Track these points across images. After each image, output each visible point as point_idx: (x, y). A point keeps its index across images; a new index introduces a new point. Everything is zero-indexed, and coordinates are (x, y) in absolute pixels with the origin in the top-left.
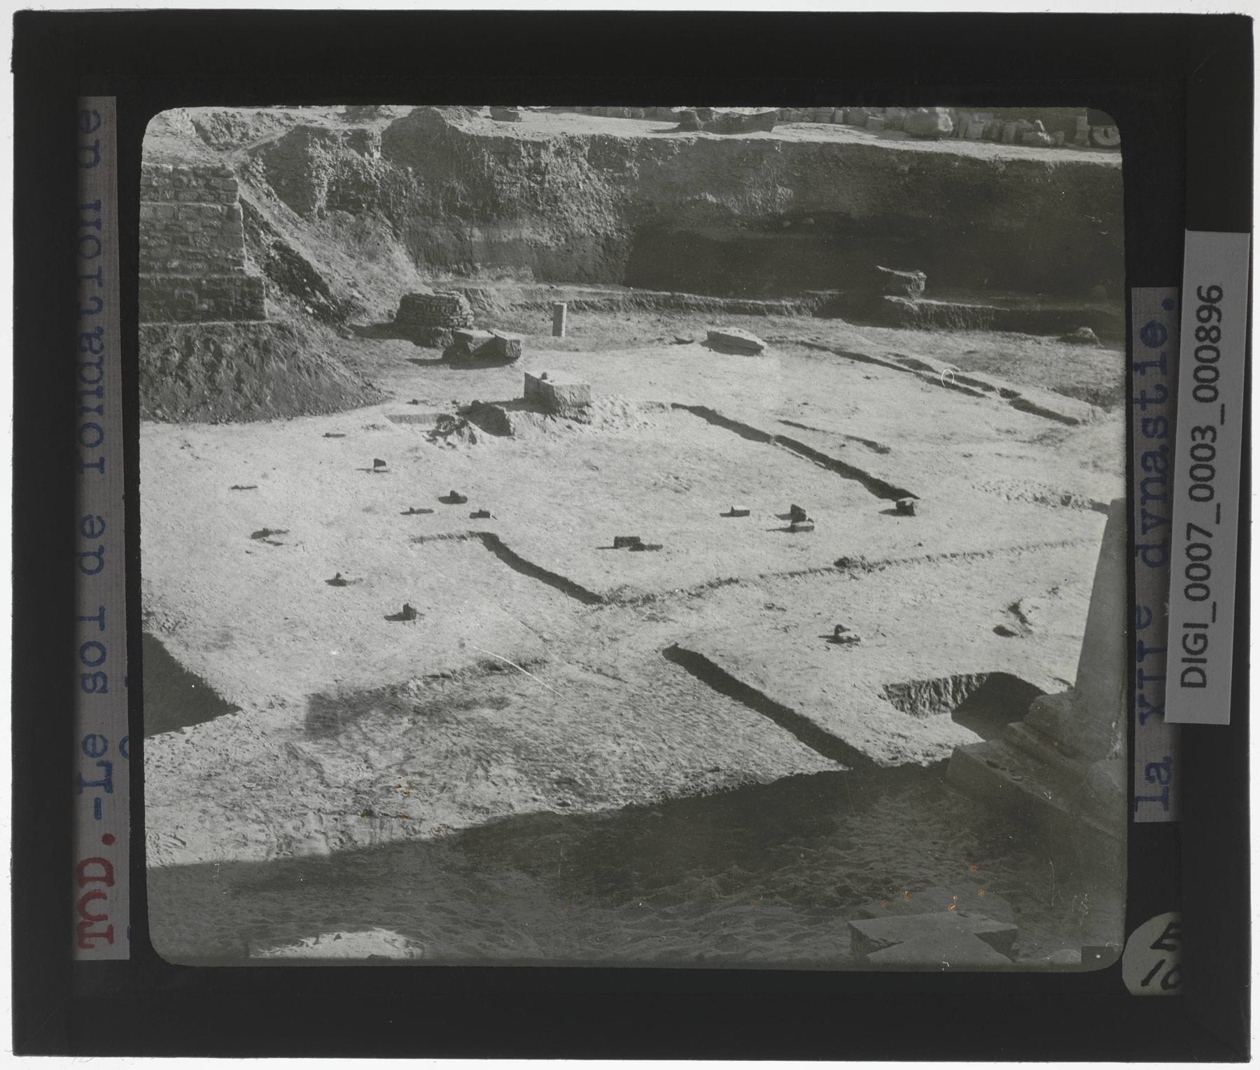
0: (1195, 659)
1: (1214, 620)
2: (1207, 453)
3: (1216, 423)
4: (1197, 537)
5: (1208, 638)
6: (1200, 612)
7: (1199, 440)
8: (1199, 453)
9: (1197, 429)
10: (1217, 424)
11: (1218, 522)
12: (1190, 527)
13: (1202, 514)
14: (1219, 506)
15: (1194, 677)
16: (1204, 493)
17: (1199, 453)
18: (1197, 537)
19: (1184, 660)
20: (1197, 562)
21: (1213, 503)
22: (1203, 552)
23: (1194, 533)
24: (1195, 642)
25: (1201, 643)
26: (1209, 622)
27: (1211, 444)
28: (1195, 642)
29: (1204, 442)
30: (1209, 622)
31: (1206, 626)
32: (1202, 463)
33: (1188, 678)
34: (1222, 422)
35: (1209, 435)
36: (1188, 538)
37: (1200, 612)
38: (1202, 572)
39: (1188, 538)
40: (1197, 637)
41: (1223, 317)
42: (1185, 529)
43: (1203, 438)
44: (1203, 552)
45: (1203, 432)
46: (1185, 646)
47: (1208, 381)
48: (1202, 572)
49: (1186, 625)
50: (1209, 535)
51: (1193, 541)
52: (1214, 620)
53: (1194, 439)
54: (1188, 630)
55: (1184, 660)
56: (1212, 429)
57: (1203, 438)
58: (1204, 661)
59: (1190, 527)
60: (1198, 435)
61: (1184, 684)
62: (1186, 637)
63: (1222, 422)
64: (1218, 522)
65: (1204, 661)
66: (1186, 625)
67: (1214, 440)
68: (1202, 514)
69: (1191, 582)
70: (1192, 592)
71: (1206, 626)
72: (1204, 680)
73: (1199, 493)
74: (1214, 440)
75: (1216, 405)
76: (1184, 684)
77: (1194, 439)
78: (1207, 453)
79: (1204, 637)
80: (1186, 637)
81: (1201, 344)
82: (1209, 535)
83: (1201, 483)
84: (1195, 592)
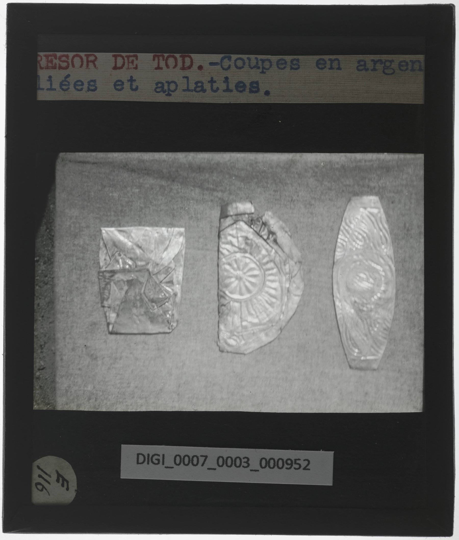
0: (149, 459)
1: (166, 467)
2: (238, 464)
3: (250, 468)
4: (202, 460)
5: (158, 465)
6: (169, 461)
7: (243, 460)
8: (238, 460)
9: (248, 459)
10: (251, 468)
11: (209, 469)
12: (206, 457)
13: (211, 462)
14: (215, 469)
15: (141, 459)
16: (221, 463)
17: (238, 460)
18: (202, 460)
19: (148, 455)
20: (191, 461)
21: (216, 466)
22: (195, 462)
23: (204, 458)
24: (156, 459)
25: (156, 462)
26: (166, 465)
27: (242, 465)
28: (156, 459)
29: (242, 462)
30: (166, 465)
31: (163, 464)
32: (234, 462)
33: (140, 456)
34: (251, 470)
35: (246, 465)
36: (201, 456)
37: (169, 461)
38: (186, 462)
39: (202, 456)
40: (158, 460)
41: (297, 471)
42: (205, 455)
43: (244, 462)
44: (195, 462)
45: (247, 462)
46: (155, 455)
47: (269, 464)
48: (186, 462)
49: (163, 455)
50: (203, 465)
51: (200, 458)
52: (166, 467)
53: (244, 458)
54: (161, 456)
55: (148, 455)
56: (249, 465)
57: (244, 462)
58: (148, 463)
59: (206, 457)
60: (246, 460)
61: (138, 455)
62: (159, 455)
63: (251, 470)
64: (209, 469)
65: (148, 463)
66: (163, 455)
67: (243, 467)
68: (211, 462)
69: (182, 457)
70: (178, 458)
71: (163, 464)
72: (141, 463)
73: (221, 461)
74: (243, 467)
75: (258, 468)
76: (138, 455)
77: (244, 458)
78: (238, 464)
79: (158, 463)
80: (159, 455)
81: (285, 461)
82: (203, 465)
83: (225, 462)
84: (178, 458)
